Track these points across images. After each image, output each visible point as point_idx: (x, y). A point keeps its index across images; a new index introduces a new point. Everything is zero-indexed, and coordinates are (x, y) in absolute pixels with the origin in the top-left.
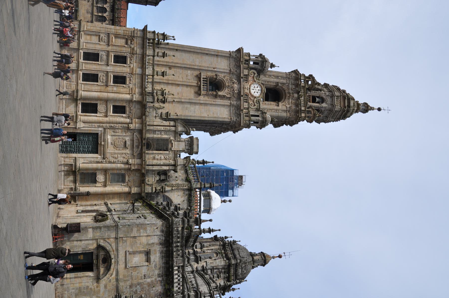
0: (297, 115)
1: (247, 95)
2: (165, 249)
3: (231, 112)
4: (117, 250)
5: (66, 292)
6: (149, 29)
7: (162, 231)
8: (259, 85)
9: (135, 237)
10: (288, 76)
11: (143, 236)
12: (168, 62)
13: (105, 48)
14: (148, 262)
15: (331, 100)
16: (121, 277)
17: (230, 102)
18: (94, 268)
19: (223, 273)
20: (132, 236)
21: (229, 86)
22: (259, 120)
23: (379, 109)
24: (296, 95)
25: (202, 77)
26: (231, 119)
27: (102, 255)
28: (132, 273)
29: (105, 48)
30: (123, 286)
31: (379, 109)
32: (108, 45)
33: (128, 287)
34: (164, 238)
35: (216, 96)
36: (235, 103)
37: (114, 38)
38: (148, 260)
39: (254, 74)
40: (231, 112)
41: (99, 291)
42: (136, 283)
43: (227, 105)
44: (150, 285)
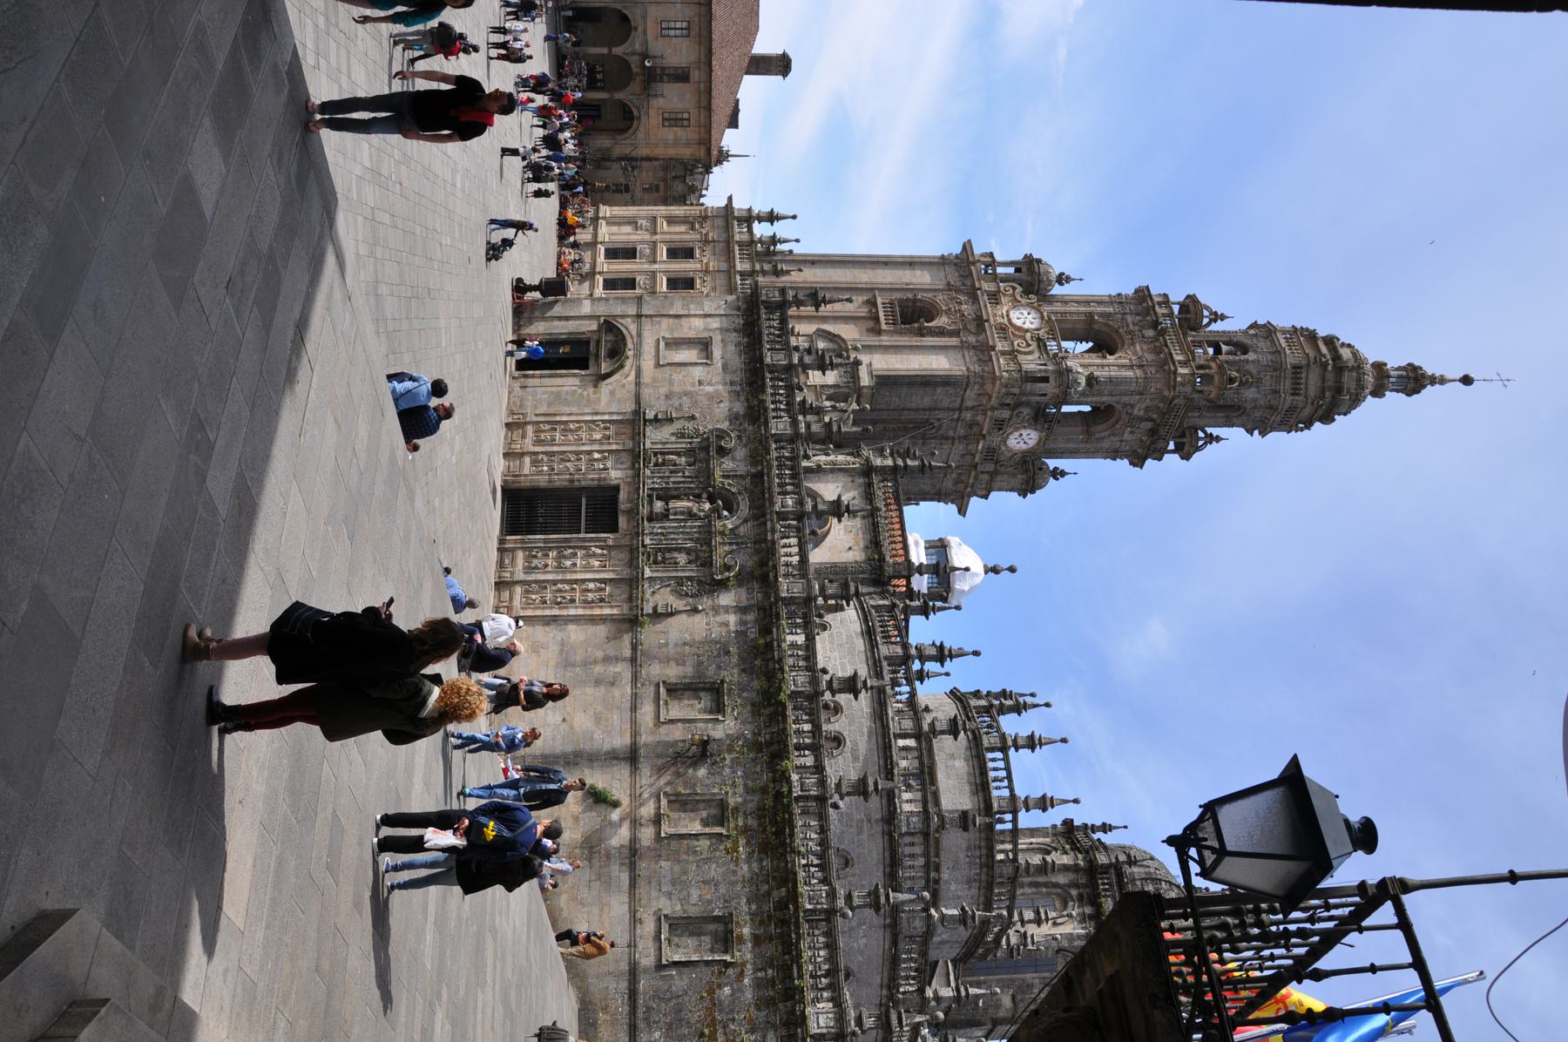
0: (1164, 370)
1: (1004, 329)
2: (746, 340)
3: (968, 360)
4: (639, 335)
5: (530, 397)
6: (736, 205)
7: (739, 309)
8: (1033, 308)
9: (678, 316)
10: (1118, 300)
11: (695, 316)
12: (795, 282)
13: (647, 237)
14: (707, 358)
15: (1269, 344)
16: (646, 378)
17: (958, 339)
18: (591, 363)
19: (1073, 901)
20: (671, 313)
21: (949, 309)
22: (1046, 371)
23: (1467, 380)
24: (1150, 333)
25: (879, 301)
26: (968, 369)
27: (610, 341)
28: (671, 375)
29: (647, 237)
30: (650, 395)
31: (1467, 380)
32: (656, 233)
33: (663, 398)
34: (742, 322)
35: (921, 333)
36: (972, 339)
37: (665, 223)
38: (709, 356)
39: (1014, 289)
40: (968, 360)
41: (599, 399)
42: (680, 391)
43: (954, 347)
44: (713, 398)
